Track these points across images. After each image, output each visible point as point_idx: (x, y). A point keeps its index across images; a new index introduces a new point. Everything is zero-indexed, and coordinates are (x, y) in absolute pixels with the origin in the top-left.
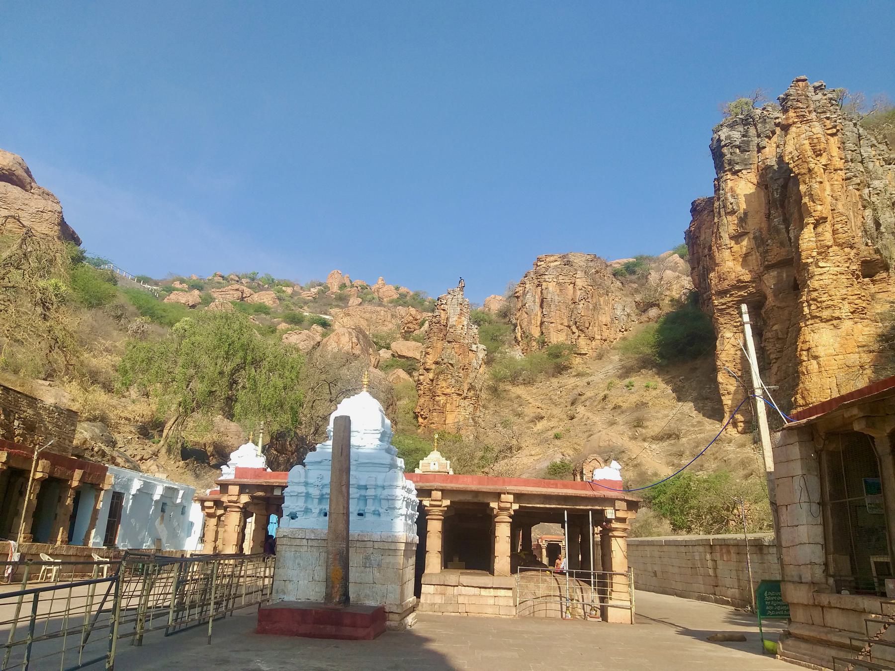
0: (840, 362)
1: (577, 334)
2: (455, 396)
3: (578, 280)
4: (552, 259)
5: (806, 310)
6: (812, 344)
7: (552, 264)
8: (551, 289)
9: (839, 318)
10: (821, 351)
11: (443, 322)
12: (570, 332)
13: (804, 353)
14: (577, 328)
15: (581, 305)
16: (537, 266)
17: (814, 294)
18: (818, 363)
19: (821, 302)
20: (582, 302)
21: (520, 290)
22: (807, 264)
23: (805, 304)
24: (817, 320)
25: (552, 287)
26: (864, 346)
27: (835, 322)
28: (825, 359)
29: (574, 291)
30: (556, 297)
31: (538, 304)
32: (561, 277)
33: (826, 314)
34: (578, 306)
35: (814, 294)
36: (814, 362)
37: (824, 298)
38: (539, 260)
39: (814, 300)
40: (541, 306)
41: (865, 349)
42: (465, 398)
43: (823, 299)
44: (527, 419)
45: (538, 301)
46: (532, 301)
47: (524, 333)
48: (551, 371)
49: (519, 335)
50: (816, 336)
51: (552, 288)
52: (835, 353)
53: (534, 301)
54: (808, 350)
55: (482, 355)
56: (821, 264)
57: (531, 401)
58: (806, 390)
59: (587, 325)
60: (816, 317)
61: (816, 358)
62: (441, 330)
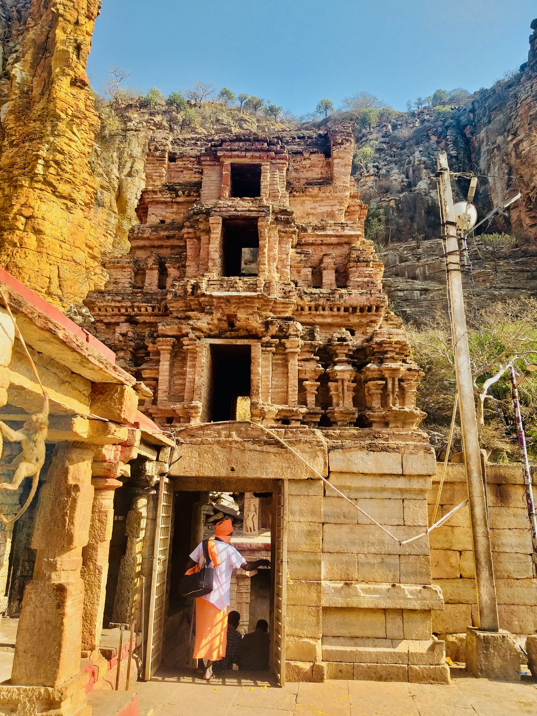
0: (66, 252)
5: (40, 169)
6: (37, 214)
9: (73, 200)
10: (46, 227)
13: (23, 220)
17: (59, 157)
18: (39, 241)
19: (63, 170)
22: (59, 118)
23: (41, 161)
24: (49, 189)
26: (90, 248)
27: (70, 204)
28: (50, 239)
33: (63, 188)
35: (59, 157)
36: (33, 237)
37: (68, 168)
39: (57, 163)
41: (91, 251)
43: (69, 170)
50: (44, 207)
52: (62, 239)
54: (28, 218)
56: (75, 129)
58: (16, 266)
60: (50, 184)
61: (38, 232)
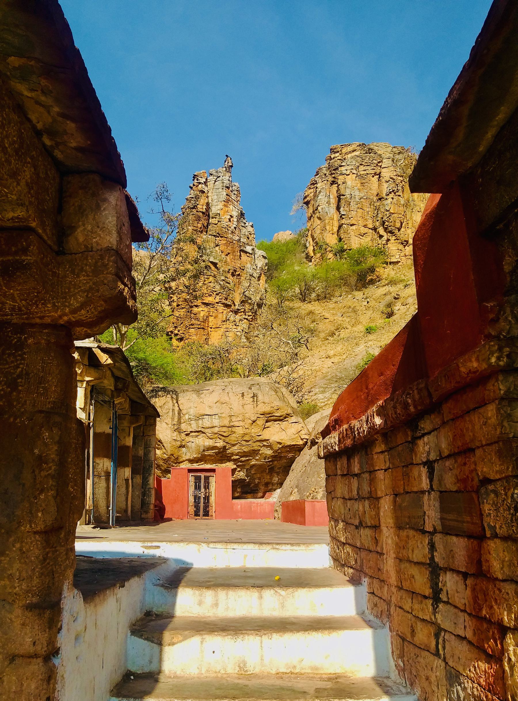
1: (385, 238)
2: (221, 308)
3: (383, 170)
4: (350, 149)
7: (349, 156)
8: (349, 183)
11: (202, 207)
12: (376, 236)
14: (386, 229)
15: (390, 200)
16: (331, 159)
20: (392, 195)
21: (310, 193)
25: (351, 181)
29: (379, 185)
30: (357, 193)
31: (334, 206)
32: (362, 168)
34: (385, 202)
38: (333, 151)
40: (338, 208)
42: (236, 312)
44: (322, 335)
45: (333, 201)
46: (326, 201)
47: (317, 243)
48: (353, 280)
49: (310, 249)
51: (350, 183)
53: (329, 203)
55: (261, 263)
57: (327, 315)
59: (398, 225)
62: (198, 219)
